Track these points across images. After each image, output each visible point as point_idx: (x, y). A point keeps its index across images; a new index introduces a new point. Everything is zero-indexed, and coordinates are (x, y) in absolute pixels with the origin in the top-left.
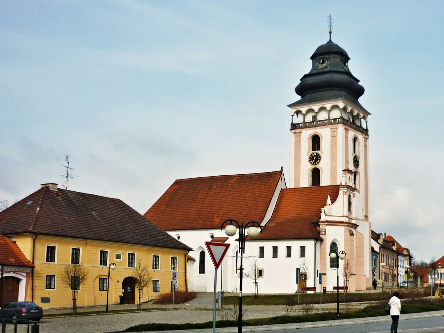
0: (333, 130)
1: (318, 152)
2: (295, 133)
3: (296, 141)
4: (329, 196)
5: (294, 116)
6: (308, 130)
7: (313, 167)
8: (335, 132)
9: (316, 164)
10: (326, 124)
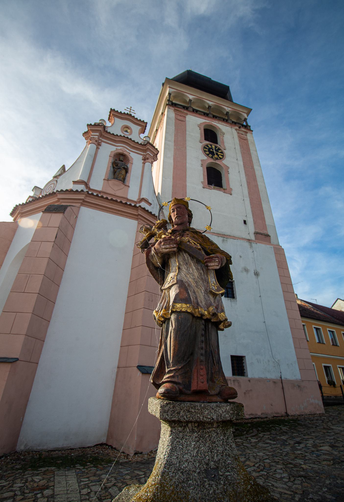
3: (176, 119)
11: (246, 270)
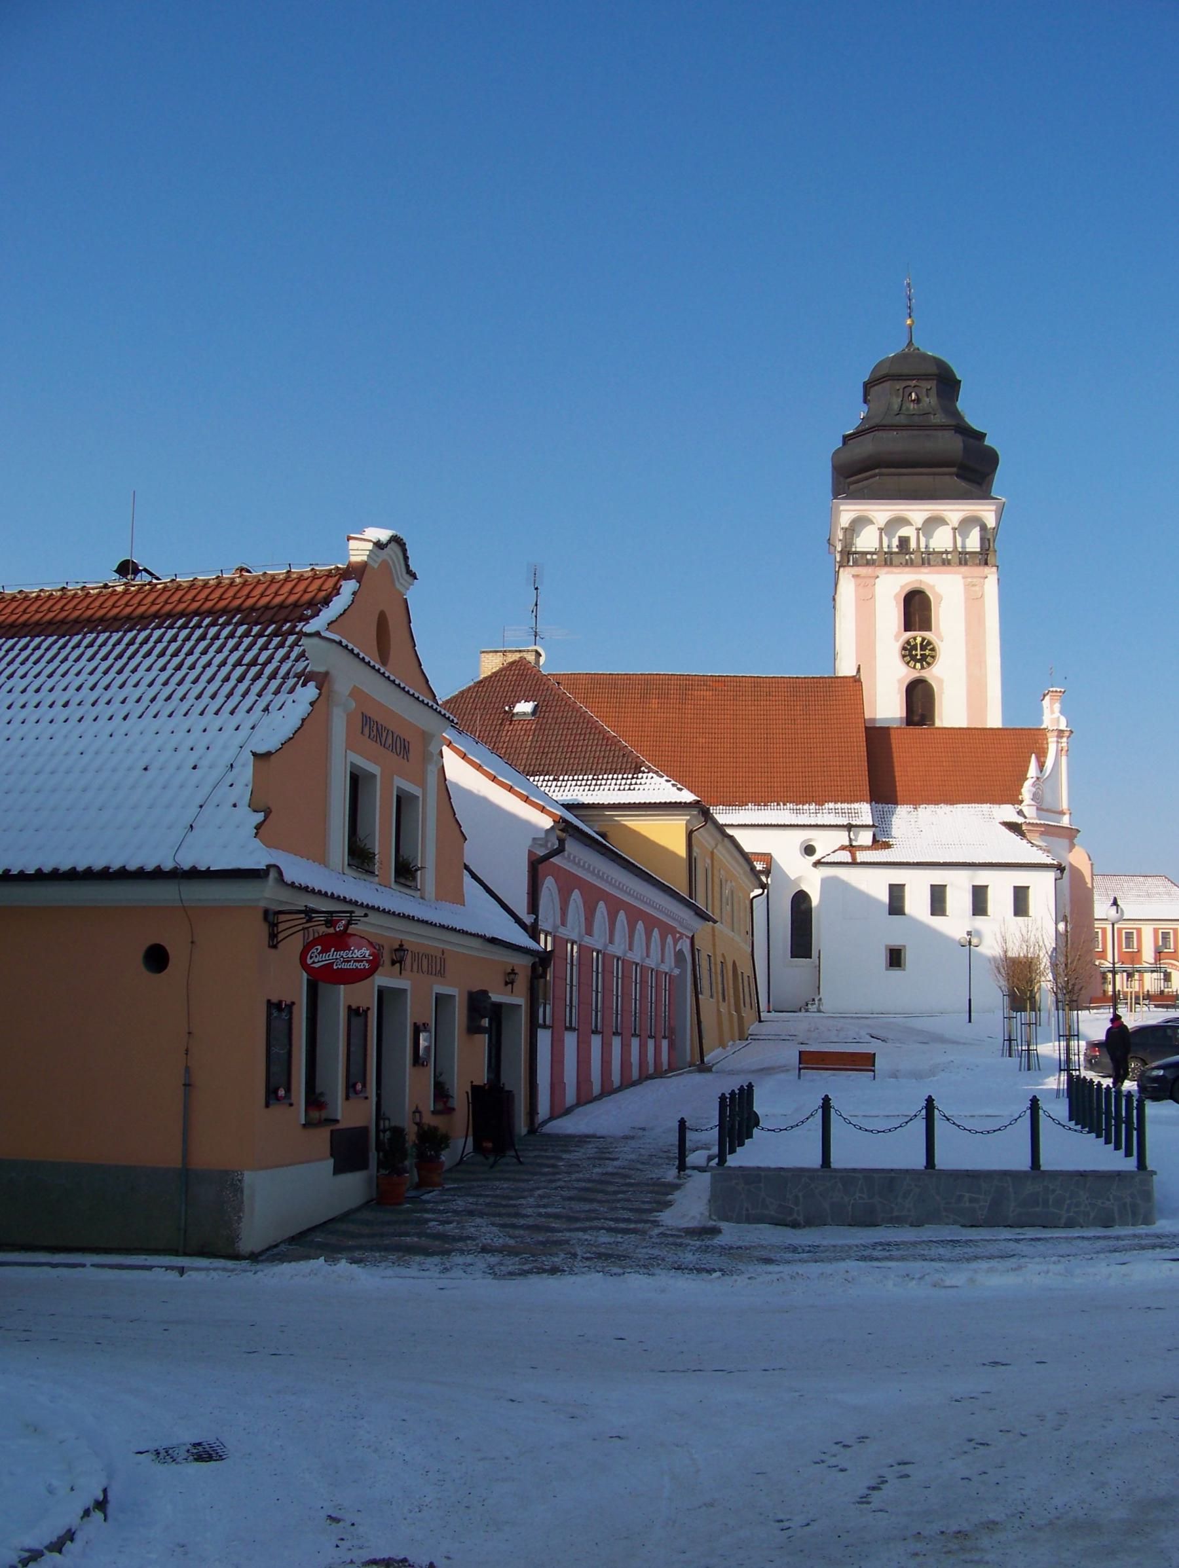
0: (969, 580)
2: (856, 576)
4: (1033, 756)
6: (895, 573)
7: (914, 675)
8: (977, 588)
9: (922, 667)
10: (946, 563)
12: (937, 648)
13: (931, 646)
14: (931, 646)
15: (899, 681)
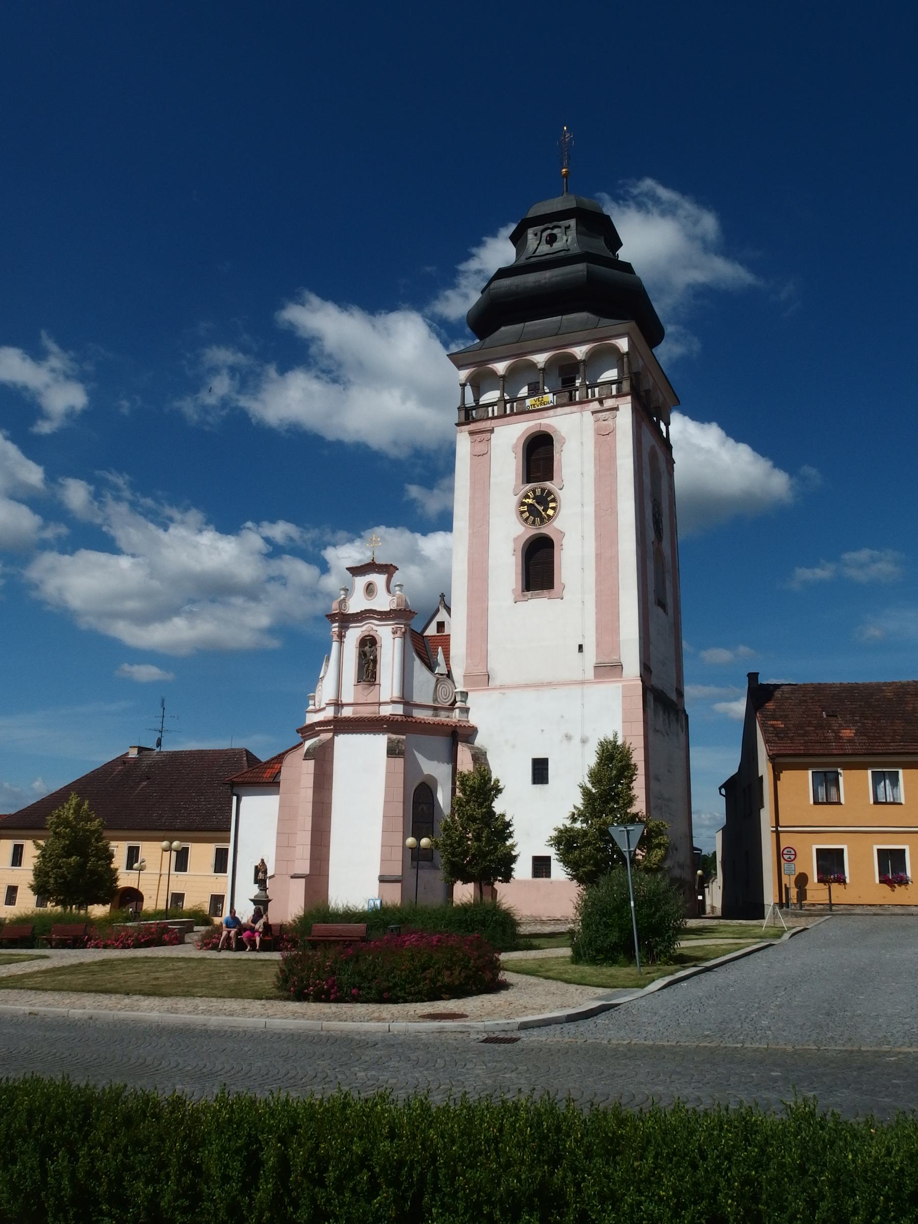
1: (548, 485)
2: (472, 433)
3: (475, 455)
5: (466, 387)
7: (532, 531)
9: (542, 521)
11: (568, 737)
12: (557, 498)
13: (553, 496)
14: (553, 496)
15: (516, 540)
